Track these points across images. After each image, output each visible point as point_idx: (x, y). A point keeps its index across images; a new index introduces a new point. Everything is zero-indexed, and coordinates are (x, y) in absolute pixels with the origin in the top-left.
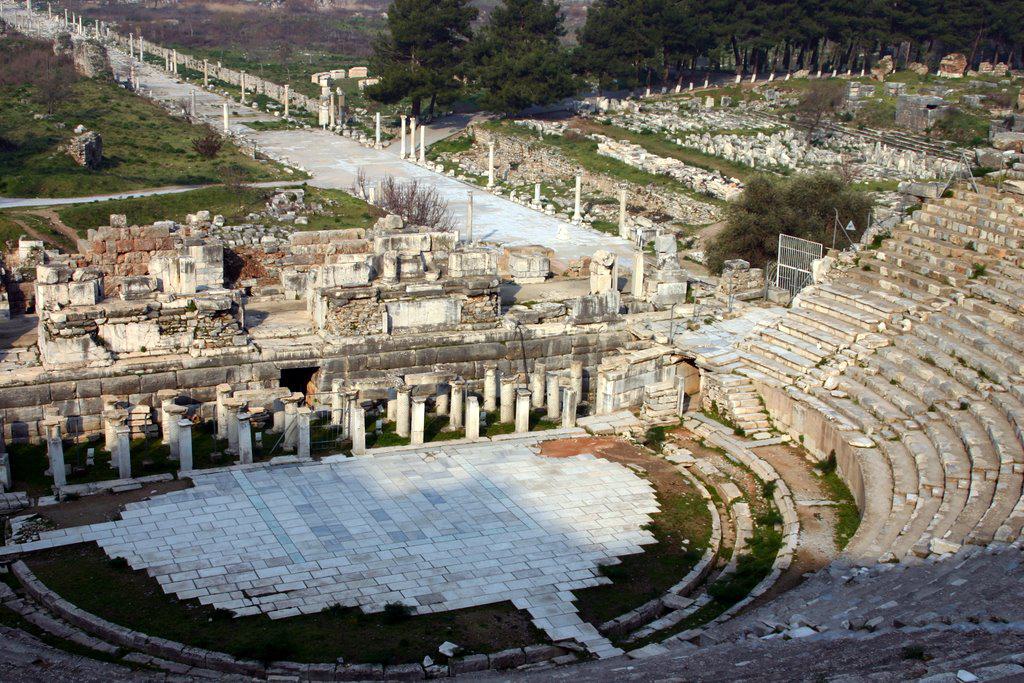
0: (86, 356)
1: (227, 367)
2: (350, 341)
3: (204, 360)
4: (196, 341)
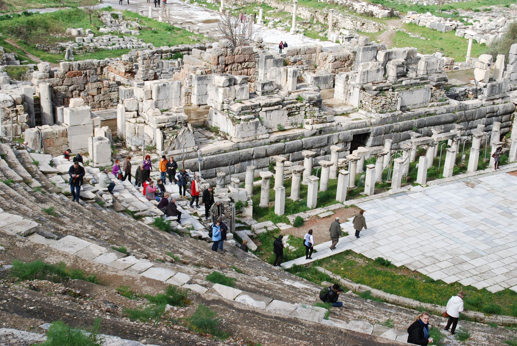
0: (256, 132)
1: (328, 135)
2: (383, 116)
3: (314, 131)
4: (308, 120)
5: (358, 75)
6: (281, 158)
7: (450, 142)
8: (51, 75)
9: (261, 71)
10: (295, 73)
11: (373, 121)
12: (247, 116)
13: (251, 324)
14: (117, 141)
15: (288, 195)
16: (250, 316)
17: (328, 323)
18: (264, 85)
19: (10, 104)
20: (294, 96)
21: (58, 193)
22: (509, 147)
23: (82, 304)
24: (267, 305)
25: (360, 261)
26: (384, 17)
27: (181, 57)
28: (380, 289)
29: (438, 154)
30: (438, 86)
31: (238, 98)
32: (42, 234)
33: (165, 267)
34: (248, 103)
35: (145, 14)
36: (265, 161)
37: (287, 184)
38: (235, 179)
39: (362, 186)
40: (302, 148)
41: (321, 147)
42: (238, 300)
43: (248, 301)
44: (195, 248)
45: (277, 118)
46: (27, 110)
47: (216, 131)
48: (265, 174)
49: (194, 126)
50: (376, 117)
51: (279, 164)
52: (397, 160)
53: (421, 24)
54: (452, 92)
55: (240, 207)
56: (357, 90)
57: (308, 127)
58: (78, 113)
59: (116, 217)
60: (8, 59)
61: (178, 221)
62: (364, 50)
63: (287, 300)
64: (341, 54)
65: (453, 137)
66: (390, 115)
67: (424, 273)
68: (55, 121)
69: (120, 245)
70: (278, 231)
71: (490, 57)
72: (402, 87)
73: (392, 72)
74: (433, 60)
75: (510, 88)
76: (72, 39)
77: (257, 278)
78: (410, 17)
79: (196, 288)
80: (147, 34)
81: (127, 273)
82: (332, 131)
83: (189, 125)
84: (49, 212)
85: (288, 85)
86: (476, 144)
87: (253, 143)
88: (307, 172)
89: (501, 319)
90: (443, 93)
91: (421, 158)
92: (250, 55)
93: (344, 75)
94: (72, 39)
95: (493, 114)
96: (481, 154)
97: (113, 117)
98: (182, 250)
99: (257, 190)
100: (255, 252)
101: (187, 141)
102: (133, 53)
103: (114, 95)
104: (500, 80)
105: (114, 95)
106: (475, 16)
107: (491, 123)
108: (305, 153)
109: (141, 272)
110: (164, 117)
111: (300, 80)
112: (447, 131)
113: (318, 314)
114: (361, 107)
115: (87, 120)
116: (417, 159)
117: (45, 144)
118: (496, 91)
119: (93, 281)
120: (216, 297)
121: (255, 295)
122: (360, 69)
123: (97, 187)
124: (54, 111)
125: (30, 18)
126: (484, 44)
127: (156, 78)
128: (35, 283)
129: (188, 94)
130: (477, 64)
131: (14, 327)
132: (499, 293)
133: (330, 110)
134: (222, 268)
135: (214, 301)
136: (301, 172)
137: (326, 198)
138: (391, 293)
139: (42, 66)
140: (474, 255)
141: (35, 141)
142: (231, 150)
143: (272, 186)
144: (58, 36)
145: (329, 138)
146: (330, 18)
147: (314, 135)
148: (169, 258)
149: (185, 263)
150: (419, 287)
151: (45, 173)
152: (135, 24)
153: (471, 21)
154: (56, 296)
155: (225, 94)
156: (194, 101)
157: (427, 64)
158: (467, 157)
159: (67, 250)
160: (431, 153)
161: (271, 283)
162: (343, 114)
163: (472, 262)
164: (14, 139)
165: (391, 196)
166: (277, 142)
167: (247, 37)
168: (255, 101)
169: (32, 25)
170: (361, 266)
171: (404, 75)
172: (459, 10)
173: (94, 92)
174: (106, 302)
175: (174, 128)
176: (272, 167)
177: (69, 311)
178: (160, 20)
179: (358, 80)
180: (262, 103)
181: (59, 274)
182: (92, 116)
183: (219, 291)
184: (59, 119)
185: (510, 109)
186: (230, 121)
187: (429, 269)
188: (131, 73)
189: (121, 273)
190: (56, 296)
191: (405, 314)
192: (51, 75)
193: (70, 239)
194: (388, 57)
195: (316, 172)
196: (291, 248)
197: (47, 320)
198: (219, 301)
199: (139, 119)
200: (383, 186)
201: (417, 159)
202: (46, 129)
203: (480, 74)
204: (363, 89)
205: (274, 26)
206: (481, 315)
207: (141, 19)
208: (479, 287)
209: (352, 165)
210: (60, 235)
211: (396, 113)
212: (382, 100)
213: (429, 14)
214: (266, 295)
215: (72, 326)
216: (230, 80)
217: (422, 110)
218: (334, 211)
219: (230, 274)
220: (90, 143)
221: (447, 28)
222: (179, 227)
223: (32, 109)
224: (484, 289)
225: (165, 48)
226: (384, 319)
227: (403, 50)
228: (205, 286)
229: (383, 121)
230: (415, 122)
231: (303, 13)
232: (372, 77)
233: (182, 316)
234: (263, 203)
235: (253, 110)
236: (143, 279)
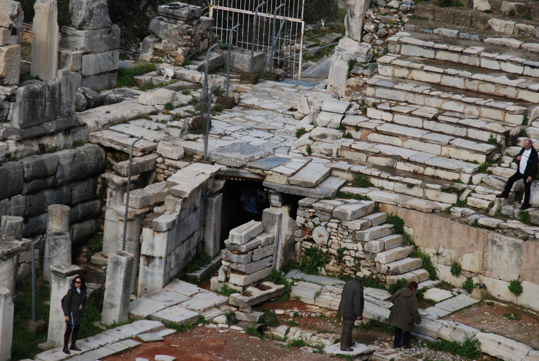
22: (101, 279)
75: (83, 101)
107: (42, 210)
185: (91, 161)
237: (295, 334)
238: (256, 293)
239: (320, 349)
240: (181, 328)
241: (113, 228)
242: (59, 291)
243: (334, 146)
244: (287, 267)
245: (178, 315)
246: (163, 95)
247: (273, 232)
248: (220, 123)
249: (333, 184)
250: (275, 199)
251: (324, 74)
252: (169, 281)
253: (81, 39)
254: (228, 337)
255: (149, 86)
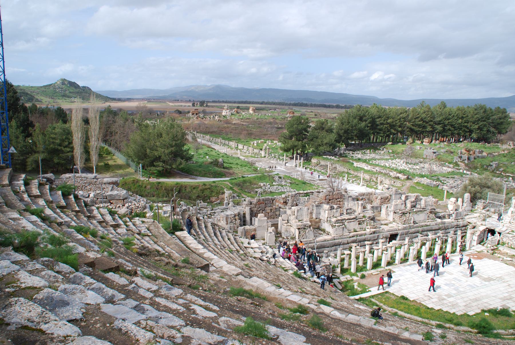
2: (405, 226)
4: (368, 227)
5: (393, 206)
6: (354, 245)
7: (437, 239)
8: (251, 203)
9: (346, 203)
10: (362, 204)
11: (400, 228)
12: (339, 224)
13: (338, 325)
14: (278, 234)
15: (358, 263)
16: (337, 321)
17: (376, 327)
18: (347, 210)
19: (233, 216)
20: (362, 215)
21: (251, 257)
23: (259, 309)
24: (346, 316)
25: (393, 297)
26: (404, 179)
27: (309, 196)
28: (402, 311)
29: (432, 245)
30: (431, 212)
31: (335, 215)
32: (243, 275)
33: (297, 295)
34: (339, 218)
35: (293, 177)
36: (347, 246)
37: (357, 258)
38: (332, 254)
39: (394, 259)
40: (365, 240)
41: (374, 240)
42: (332, 313)
43: (337, 314)
44: (312, 287)
45: (353, 225)
46: (240, 219)
47: (324, 231)
48: (347, 252)
49: (314, 228)
50: (401, 226)
51: (353, 248)
52: (411, 248)
53: (422, 183)
54: (437, 215)
55: (334, 268)
56: (392, 213)
57: (368, 230)
58: (261, 220)
59: (276, 270)
60: (234, 196)
61: (305, 273)
62: (395, 194)
63: (356, 315)
64: (384, 196)
65: (438, 237)
66: (408, 225)
67: (425, 304)
68: (251, 224)
69: (278, 283)
70: (352, 280)
71: (455, 199)
72: (414, 212)
73: (409, 205)
74: (428, 200)
76: (261, 187)
77: (341, 303)
78: (416, 179)
79: (312, 306)
80: (293, 186)
81: (280, 296)
82: (379, 232)
83: (311, 228)
84: (247, 265)
85: (358, 210)
86: (450, 240)
87: (341, 237)
88: (367, 252)
89: (462, 328)
90: (433, 215)
91: (423, 247)
92: (341, 196)
93: (386, 206)
94: (261, 187)
95: (457, 226)
96: (452, 245)
97: (276, 223)
98: (306, 287)
99: (342, 260)
100: (341, 290)
101: (310, 235)
102: (287, 194)
103: (277, 213)
104: (460, 210)
105: (277, 213)
106: (447, 180)
107: (457, 231)
108: (366, 243)
109: (286, 297)
110: (300, 223)
111: (364, 208)
112: (436, 234)
113: (371, 322)
114: (394, 221)
115: (265, 224)
116: (421, 247)
117: (246, 234)
118: (459, 216)
119: (264, 299)
120: (321, 311)
121: (340, 311)
122: (393, 203)
123: (268, 255)
124: (251, 220)
125: (244, 179)
126: (452, 193)
127: (297, 205)
128: (239, 297)
129: (311, 213)
130: (449, 202)
131: (230, 317)
132: (461, 315)
133: (379, 222)
134: (325, 297)
135: (320, 313)
136: (364, 252)
137: (376, 265)
138: (408, 313)
139: (247, 199)
140: (449, 296)
141: (242, 232)
142: (331, 240)
143: (350, 258)
144: (255, 186)
145: (378, 236)
146: (379, 179)
147: (371, 234)
148: (300, 291)
149: (307, 294)
150: (422, 311)
151: (246, 248)
152: (289, 181)
153: (445, 182)
154: (247, 304)
155: (328, 213)
156: (314, 216)
157: (426, 202)
158: (446, 247)
159: (253, 284)
160: (428, 245)
161: (348, 305)
162: (385, 224)
163: (448, 299)
164: (234, 232)
165: (408, 265)
166: (353, 237)
167: (339, 187)
168: (343, 217)
169: (245, 182)
170: (393, 299)
171: (415, 207)
172: (440, 177)
173: (269, 211)
174: (270, 309)
175: (304, 229)
176: (350, 249)
177: (253, 313)
178: (300, 179)
179: (392, 208)
180: (346, 218)
181: (250, 295)
182: (267, 222)
183: (323, 308)
184: (253, 223)
185: (465, 224)
186: (330, 226)
187: (427, 302)
188: (285, 203)
189: (277, 297)
190: (247, 304)
191: (414, 324)
192: (251, 203)
193: (255, 278)
194: (407, 198)
195: (372, 252)
196: (358, 289)
197: (244, 316)
198: (323, 313)
199: (288, 224)
200: (404, 260)
201: (421, 247)
202: (247, 227)
203: (451, 207)
204: (395, 213)
205: (353, 182)
206: (452, 326)
207: (291, 179)
208: (452, 312)
209: (389, 249)
210: (251, 277)
211: (411, 225)
212: (404, 218)
213: (425, 178)
214: (345, 311)
215: (255, 320)
216: (331, 207)
217: (423, 224)
218: (380, 271)
219: (329, 300)
220: (266, 234)
221: (434, 185)
222: (305, 276)
223: (242, 218)
224: (454, 313)
225: (301, 192)
226: (404, 326)
227: (414, 194)
228: (316, 305)
229: (404, 228)
230: (420, 229)
231: (366, 176)
232: (399, 207)
233: (305, 319)
234: (346, 266)
235: (342, 221)
236: (287, 300)
237: (499, 255)
238: (492, 248)
239: (503, 258)
240: (479, 252)
241: (468, 235)
242: (459, 244)
243: (508, 225)
244: (498, 244)
245: (478, 250)
246: (478, 214)
247: (496, 238)
248: (488, 220)
249: (507, 231)
250: (497, 233)
251: (507, 213)
252: (477, 244)
253: (465, 205)
254: (487, 255)
255: (476, 213)
